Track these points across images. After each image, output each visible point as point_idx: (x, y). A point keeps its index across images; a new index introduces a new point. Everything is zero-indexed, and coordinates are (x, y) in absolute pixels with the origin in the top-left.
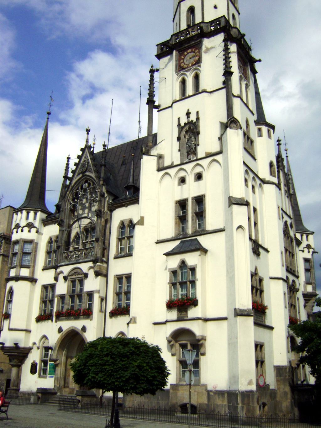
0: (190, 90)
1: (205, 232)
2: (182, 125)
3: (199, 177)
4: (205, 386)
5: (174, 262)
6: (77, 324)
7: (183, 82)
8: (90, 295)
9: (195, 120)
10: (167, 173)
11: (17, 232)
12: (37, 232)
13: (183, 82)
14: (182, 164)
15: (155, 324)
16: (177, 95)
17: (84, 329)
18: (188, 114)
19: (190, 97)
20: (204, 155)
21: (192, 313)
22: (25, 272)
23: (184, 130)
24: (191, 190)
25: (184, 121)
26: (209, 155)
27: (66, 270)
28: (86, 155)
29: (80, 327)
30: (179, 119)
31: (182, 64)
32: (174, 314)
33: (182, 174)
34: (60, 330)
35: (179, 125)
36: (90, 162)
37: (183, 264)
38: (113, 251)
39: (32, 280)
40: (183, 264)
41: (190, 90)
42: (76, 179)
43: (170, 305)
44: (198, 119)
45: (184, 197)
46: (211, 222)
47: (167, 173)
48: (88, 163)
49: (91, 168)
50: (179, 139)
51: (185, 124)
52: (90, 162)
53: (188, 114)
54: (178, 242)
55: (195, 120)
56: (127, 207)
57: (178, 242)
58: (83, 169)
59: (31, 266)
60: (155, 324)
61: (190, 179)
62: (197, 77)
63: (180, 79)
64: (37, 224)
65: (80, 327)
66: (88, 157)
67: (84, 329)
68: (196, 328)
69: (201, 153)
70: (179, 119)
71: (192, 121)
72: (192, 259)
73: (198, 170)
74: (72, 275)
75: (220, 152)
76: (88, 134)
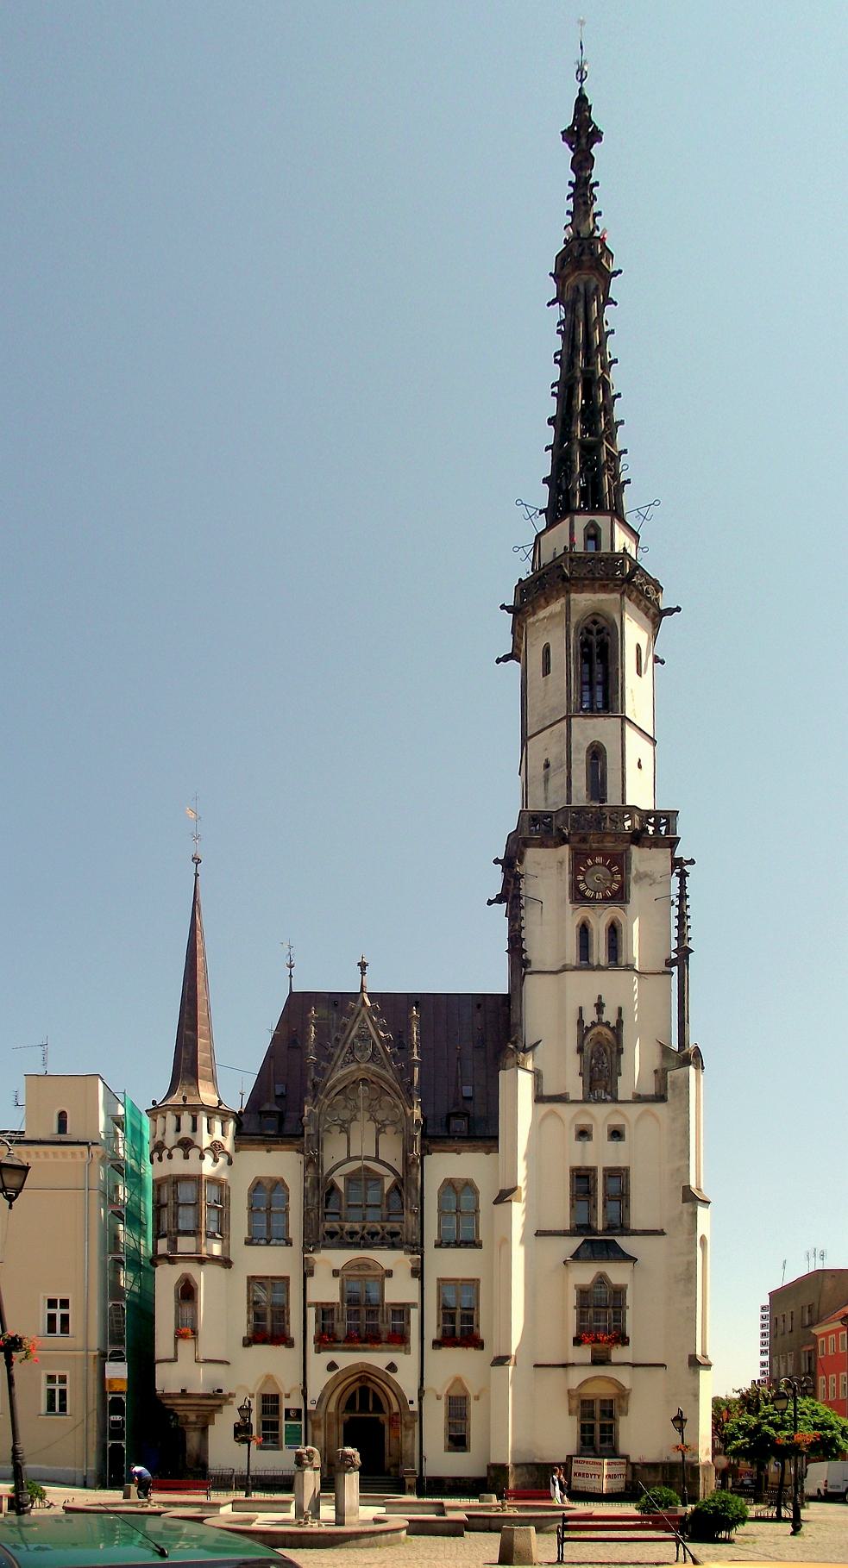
0: (600, 952)
1: (625, 1231)
2: (587, 1023)
3: (616, 1134)
4: (626, 1457)
5: (585, 1274)
6: (377, 1359)
7: (584, 931)
8: (401, 1311)
9: (613, 1024)
10: (553, 1112)
11: (186, 1157)
12: (230, 1162)
13: (584, 931)
14: (585, 1101)
15: (536, 1366)
16: (572, 955)
17: (392, 1367)
18: (600, 1006)
19: (599, 968)
20: (630, 1098)
21: (618, 1354)
22: (216, 1249)
23: (590, 1036)
24: (600, 1154)
25: (590, 1016)
26: (639, 1099)
27: (339, 1257)
28: (363, 1021)
29: (382, 1366)
30: (581, 1009)
31: (582, 886)
32: (584, 1353)
33: (584, 1121)
34: (332, 1366)
35: (580, 1022)
37: (601, 1280)
38: (431, 1234)
39: (226, 1262)
40: (601, 1280)
41: (600, 952)
43: (577, 1341)
44: (620, 1022)
45: (590, 1164)
46: (640, 1216)
47: (553, 1112)
50: (580, 1050)
51: (594, 1024)
53: (600, 1006)
54: (577, 1242)
55: (613, 1024)
57: (577, 1242)
59: (222, 1233)
60: (536, 1366)
61: (600, 1133)
62: (614, 931)
63: (577, 920)
64: (228, 1144)
65: (382, 1366)
67: (392, 1367)
68: (624, 1377)
69: (625, 1089)
70: (581, 1009)
71: (607, 1024)
72: (617, 1274)
73: (616, 1121)
74: (352, 1268)
75: (660, 1098)
76: (363, 974)
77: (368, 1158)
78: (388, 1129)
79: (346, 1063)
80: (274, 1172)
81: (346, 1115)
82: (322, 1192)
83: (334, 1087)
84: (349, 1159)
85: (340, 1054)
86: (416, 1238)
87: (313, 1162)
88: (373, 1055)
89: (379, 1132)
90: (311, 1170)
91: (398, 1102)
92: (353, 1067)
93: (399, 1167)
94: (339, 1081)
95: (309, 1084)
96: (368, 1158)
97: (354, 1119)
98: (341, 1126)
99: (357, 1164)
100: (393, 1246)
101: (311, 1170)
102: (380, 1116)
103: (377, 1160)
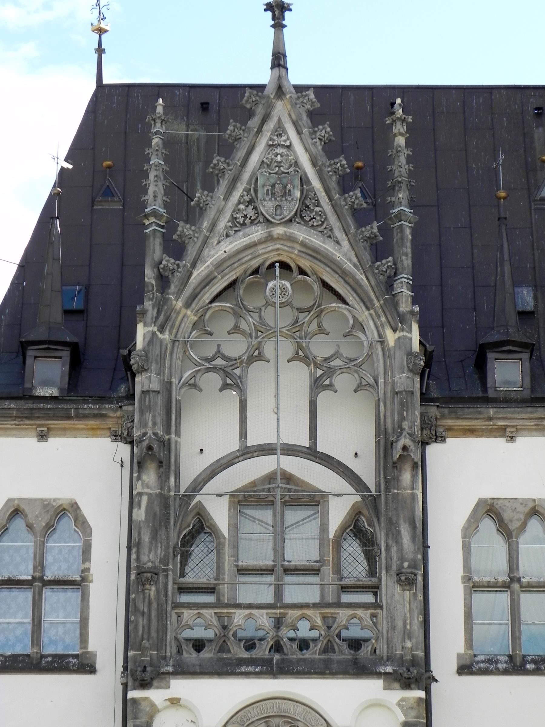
28: (280, 131)
36: (316, 184)
42: (229, 246)
48: (304, 181)
49: (322, 213)
52: (316, 184)
56: (512, 439)
58: (278, 207)
66: (289, 147)
76: (278, 25)
77: (290, 450)
78: (339, 380)
79: (238, 225)
80: (58, 491)
81: (236, 347)
82: (169, 527)
83: (208, 281)
84: (247, 452)
85: (224, 205)
86: (411, 646)
87: (154, 455)
88: (304, 207)
89: (318, 386)
90: (150, 477)
91: (364, 315)
92: (257, 233)
93: (366, 469)
94: (220, 266)
95: (150, 275)
96: (290, 450)
97: (256, 356)
98: (225, 372)
99: (263, 466)
100: (359, 669)
101: (150, 477)
102: (321, 348)
103: (312, 453)
